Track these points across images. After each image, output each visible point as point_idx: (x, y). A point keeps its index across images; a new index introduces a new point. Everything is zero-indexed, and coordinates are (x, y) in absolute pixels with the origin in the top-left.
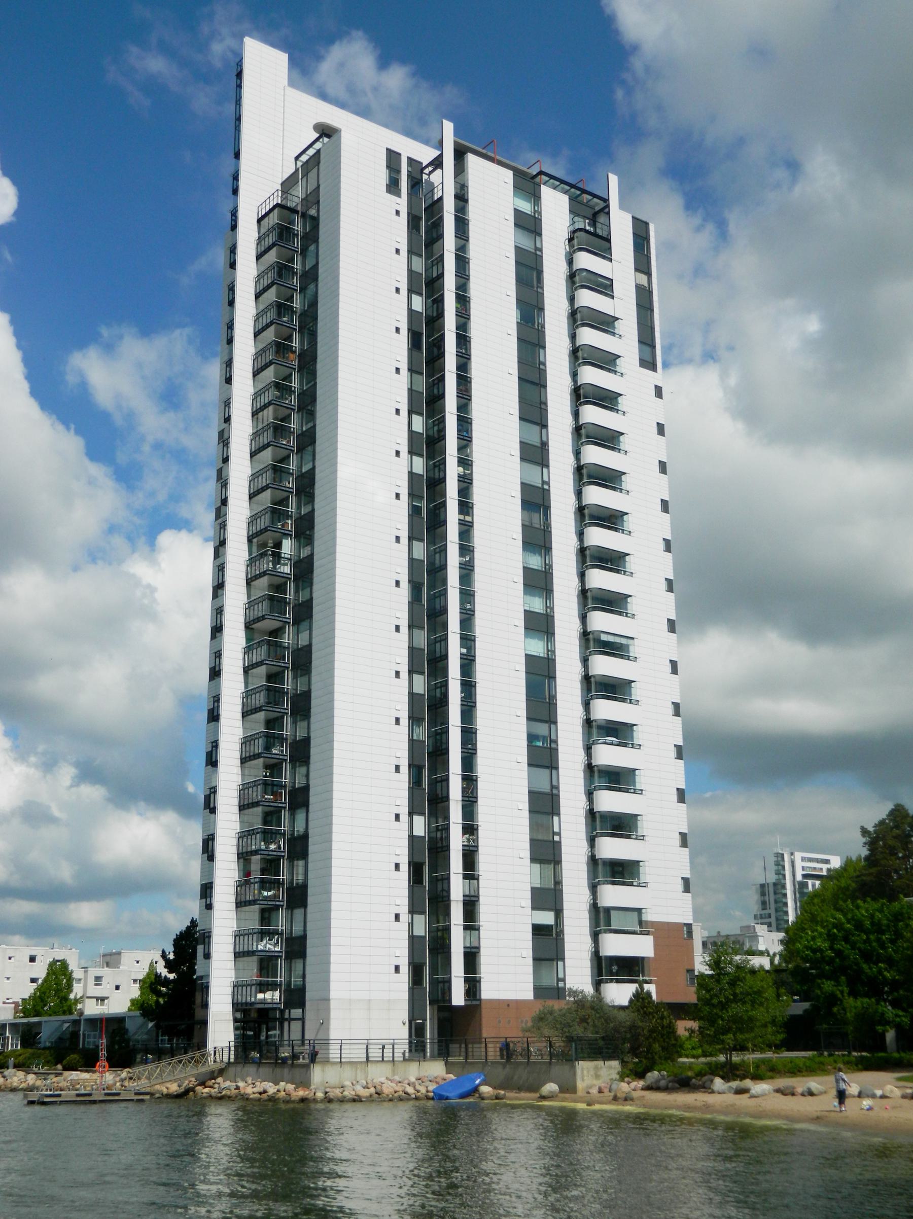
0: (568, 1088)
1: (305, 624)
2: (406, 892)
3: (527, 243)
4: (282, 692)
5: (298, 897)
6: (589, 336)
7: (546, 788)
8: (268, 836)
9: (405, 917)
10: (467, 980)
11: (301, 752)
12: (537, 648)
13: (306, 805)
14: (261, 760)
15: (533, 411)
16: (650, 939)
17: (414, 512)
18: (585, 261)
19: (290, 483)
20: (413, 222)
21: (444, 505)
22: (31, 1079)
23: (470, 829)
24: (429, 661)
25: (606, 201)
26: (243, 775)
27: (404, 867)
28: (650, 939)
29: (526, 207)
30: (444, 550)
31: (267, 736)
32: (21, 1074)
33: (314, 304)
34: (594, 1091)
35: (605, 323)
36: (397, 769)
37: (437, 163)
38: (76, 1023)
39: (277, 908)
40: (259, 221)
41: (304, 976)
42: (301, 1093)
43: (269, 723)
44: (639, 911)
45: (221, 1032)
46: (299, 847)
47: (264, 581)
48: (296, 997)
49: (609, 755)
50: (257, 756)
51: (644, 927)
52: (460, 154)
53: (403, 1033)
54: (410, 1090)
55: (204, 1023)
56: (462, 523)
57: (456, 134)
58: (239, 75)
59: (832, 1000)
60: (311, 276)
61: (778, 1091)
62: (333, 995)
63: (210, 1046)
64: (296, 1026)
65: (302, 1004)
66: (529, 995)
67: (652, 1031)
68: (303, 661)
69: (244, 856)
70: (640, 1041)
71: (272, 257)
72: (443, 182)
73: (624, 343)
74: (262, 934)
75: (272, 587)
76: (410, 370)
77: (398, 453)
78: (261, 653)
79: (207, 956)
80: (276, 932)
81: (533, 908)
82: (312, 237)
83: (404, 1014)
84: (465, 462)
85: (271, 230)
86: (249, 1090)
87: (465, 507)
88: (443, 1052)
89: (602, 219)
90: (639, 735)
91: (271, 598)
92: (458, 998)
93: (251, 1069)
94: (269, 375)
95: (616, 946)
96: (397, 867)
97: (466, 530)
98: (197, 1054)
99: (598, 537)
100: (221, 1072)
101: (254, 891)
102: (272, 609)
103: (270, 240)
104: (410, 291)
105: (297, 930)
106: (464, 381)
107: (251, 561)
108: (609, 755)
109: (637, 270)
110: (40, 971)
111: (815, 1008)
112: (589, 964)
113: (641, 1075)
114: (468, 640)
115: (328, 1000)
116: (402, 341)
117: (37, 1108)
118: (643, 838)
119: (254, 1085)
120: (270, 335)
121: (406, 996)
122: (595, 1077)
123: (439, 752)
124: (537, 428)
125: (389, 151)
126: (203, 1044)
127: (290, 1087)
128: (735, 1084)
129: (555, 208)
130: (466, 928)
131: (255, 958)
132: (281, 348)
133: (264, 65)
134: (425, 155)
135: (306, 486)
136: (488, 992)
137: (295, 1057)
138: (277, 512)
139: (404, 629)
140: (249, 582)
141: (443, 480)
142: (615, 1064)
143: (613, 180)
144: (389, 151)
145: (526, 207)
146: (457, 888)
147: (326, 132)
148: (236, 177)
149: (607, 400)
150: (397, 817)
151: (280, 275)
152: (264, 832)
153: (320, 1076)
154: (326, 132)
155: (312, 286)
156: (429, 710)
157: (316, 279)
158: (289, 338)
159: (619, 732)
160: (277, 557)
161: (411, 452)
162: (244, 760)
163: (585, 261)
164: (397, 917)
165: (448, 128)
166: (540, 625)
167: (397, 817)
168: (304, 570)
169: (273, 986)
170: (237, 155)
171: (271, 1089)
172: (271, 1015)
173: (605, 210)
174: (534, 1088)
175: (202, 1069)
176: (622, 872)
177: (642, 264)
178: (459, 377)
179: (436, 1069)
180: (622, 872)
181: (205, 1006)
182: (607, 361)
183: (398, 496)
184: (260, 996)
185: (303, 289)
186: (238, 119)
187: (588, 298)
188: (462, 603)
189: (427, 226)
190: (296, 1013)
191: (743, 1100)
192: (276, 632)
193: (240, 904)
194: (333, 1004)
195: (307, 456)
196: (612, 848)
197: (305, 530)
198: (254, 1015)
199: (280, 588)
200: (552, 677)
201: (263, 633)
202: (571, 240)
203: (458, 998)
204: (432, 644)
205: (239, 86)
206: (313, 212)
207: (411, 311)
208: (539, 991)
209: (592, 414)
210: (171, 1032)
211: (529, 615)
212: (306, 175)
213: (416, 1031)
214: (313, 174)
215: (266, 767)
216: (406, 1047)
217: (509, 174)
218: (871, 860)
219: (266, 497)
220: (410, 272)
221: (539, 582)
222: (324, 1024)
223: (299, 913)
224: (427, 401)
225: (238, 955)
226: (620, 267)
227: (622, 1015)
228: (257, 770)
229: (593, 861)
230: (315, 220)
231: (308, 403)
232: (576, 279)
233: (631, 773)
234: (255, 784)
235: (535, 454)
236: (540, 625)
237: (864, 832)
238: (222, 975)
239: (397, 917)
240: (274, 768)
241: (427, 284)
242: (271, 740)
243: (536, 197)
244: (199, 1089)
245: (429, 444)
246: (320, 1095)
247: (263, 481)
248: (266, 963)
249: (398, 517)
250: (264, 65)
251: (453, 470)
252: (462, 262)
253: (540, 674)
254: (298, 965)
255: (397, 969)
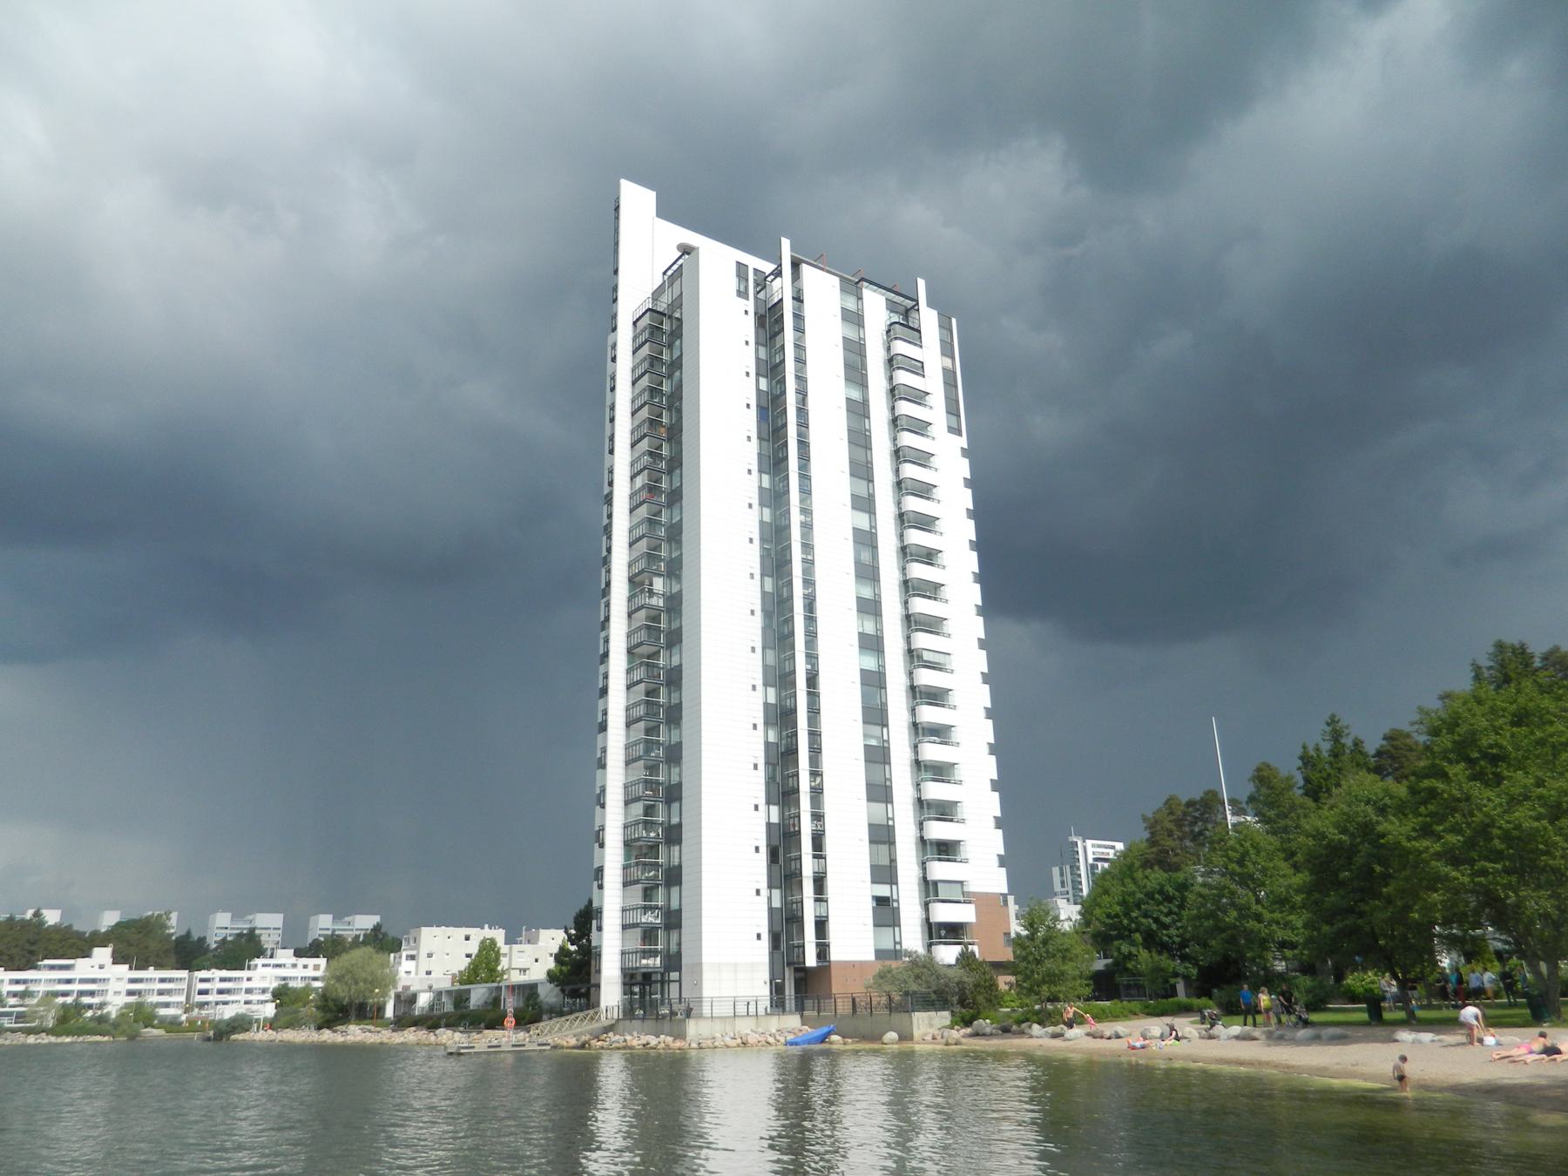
0: (906, 1037)
1: (675, 650)
2: (764, 871)
3: (853, 335)
4: (658, 704)
5: (674, 877)
6: (905, 408)
7: (879, 780)
8: (648, 825)
9: (765, 892)
10: (818, 945)
11: (674, 755)
12: (870, 663)
13: (680, 799)
14: (641, 763)
15: (861, 470)
16: (971, 908)
17: (765, 556)
18: (900, 347)
19: (662, 532)
20: (760, 321)
21: (789, 547)
22: (458, 1036)
23: (818, 817)
24: (779, 677)
25: (917, 301)
26: (626, 775)
27: (763, 850)
28: (971, 908)
29: (851, 304)
30: (790, 583)
31: (647, 741)
32: (449, 1032)
33: (680, 387)
34: (929, 1038)
35: (919, 397)
36: (756, 767)
37: (778, 273)
38: (499, 989)
39: (657, 886)
40: (635, 323)
41: (679, 944)
42: (678, 1044)
43: (648, 731)
44: (961, 883)
45: (611, 993)
46: (674, 835)
47: (642, 613)
48: (673, 961)
49: (932, 752)
50: (639, 758)
51: (967, 898)
52: (796, 265)
53: (765, 991)
54: (771, 1040)
55: (598, 986)
56: (804, 561)
57: (792, 250)
58: (617, 209)
59: (1130, 957)
60: (677, 364)
61: (1088, 1034)
62: (705, 960)
63: (603, 1005)
64: (674, 987)
65: (679, 969)
66: (871, 957)
67: (976, 986)
68: (674, 678)
69: (628, 844)
70: (966, 997)
71: (645, 350)
72: (782, 288)
73: (935, 412)
74: (646, 909)
75: (649, 618)
76: (759, 438)
77: (750, 506)
78: (639, 674)
79: (600, 929)
80: (656, 907)
81: (873, 882)
82: (677, 333)
83: (765, 974)
84: (807, 511)
85: (643, 331)
86: (635, 1043)
87: (807, 547)
88: (800, 1008)
89: (913, 314)
90: (956, 735)
91: (648, 627)
92: (811, 960)
93: (637, 1023)
94: (644, 445)
95: (944, 913)
96: (757, 849)
97: (809, 564)
98: (591, 1012)
99: (918, 571)
100: (609, 1029)
101: (636, 873)
102: (649, 636)
103: (642, 339)
104: (758, 374)
105: (674, 905)
106: (803, 445)
107: (630, 599)
108: (932, 752)
109: (943, 354)
110: (473, 947)
111: (1116, 964)
112: (919, 929)
113: (967, 1023)
114: (812, 658)
115: (700, 964)
116: (751, 416)
117: (452, 1061)
118: (963, 821)
119: (639, 1038)
120: (644, 413)
121: (766, 959)
122: (929, 1026)
123: (791, 753)
124: (865, 483)
125: (738, 263)
126: (598, 1005)
127: (670, 1039)
128: (1051, 1029)
129: (875, 305)
130: (816, 900)
131: (639, 930)
132: (653, 423)
133: (637, 201)
134: (767, 267)
135: (675, 534)
136: (836, 955)
137: (673, 1014)
138: (651, 557)
139: (759, 650)
140: (630, 615)
141: (789, 526)
142: (946, 1014)
143: (921, 283)
144: (738, 263)
145: (851, 304)
146: (808, 867)
147: (686, 250)
148: (615, 289)
149: (923, 459)
150: (756, 808)
151: (652, 365)
152: (646, 822)
153: (693, 1028)
154: (686, 250)
155: (677, 374)
156: (781, 716)
157: (681, 367)
158: (660, 416)
159: (940, 733)
160: (651, 593)
161: (762, 504)
162: (628, 763)
163: (900, 347)
164: (758, 892)
165: (786, 244)
166: (872, 643)
167: (756, 808)
168: (674, 603)
169: (654, 954)
170: (616, 272)
171: (653, 1041)
172: (654, 978)
173: (916, 307)
174: (877, 1037)
175: (596, 1025)
176: (947, 850)
177: (947, 350)
178: (800, 442)
179: (793, 1021)
180: (947, 850)
181: (599, 971)
182: (920, 428)
183: (751, 541)
184: (644, 962)
185: (670, 376)
186: (617, 244)
187: (903, 377)
188: (806, 627)
189: (769, 322)
190: (674, 975)
191: (1057, 1043)
192: (656, 655)
193: (625, 884)
194: (705, 968)
195: (676, 511)
196: (938, 830)
197: (674, 571)
198: (639, 978)
199: (656, 619)
200: (882, 685)
201: (642, 656)
202: (888, 332)
203: (811, 960)
204: (781, 662)
205: (617, 218)
206: (677, 315)
207: (758, 390)
208: (879, 954)
209: (910, 471)
210: (574, 994)
211: (862, 636)
212: (671, 285)
213: (777, 990)
214: (677, 285)
215: (646, 768)
216: (768, 1003)
217: (835, 281)
218: (1153, 842)
219: (643, 545)
220: (758, 359)
221: (870, 608)
222: (698, 984)
223: (675, 891)
224: (773, 460)
225: (624, 927)
226: (930, 351)
227: (951, 973)
228: (639, 771)
229: (922, 841)
230: (680, 320)
231: (676, 463)
232: (891, 362)
233: (939, 621)
234: (638, 782)
235: (864, 503)
236: (872, 643)
237: (1145, 819)
238: (612, 948)
239: (758, 892)
240: (652, 769)
241: (771, 369)
242: (649, 745)
243: (860, 298)
244: (594, 1042)
245: (775, 498)
246: (694, 1045)
247: (639, 532)
248: (649, 934)
249: (752, 557)
250: (637, 201)
251: (796, 518)
252: (800, 347)
253: (873, 682)
254: (674, 936)
255: (759, 936)
